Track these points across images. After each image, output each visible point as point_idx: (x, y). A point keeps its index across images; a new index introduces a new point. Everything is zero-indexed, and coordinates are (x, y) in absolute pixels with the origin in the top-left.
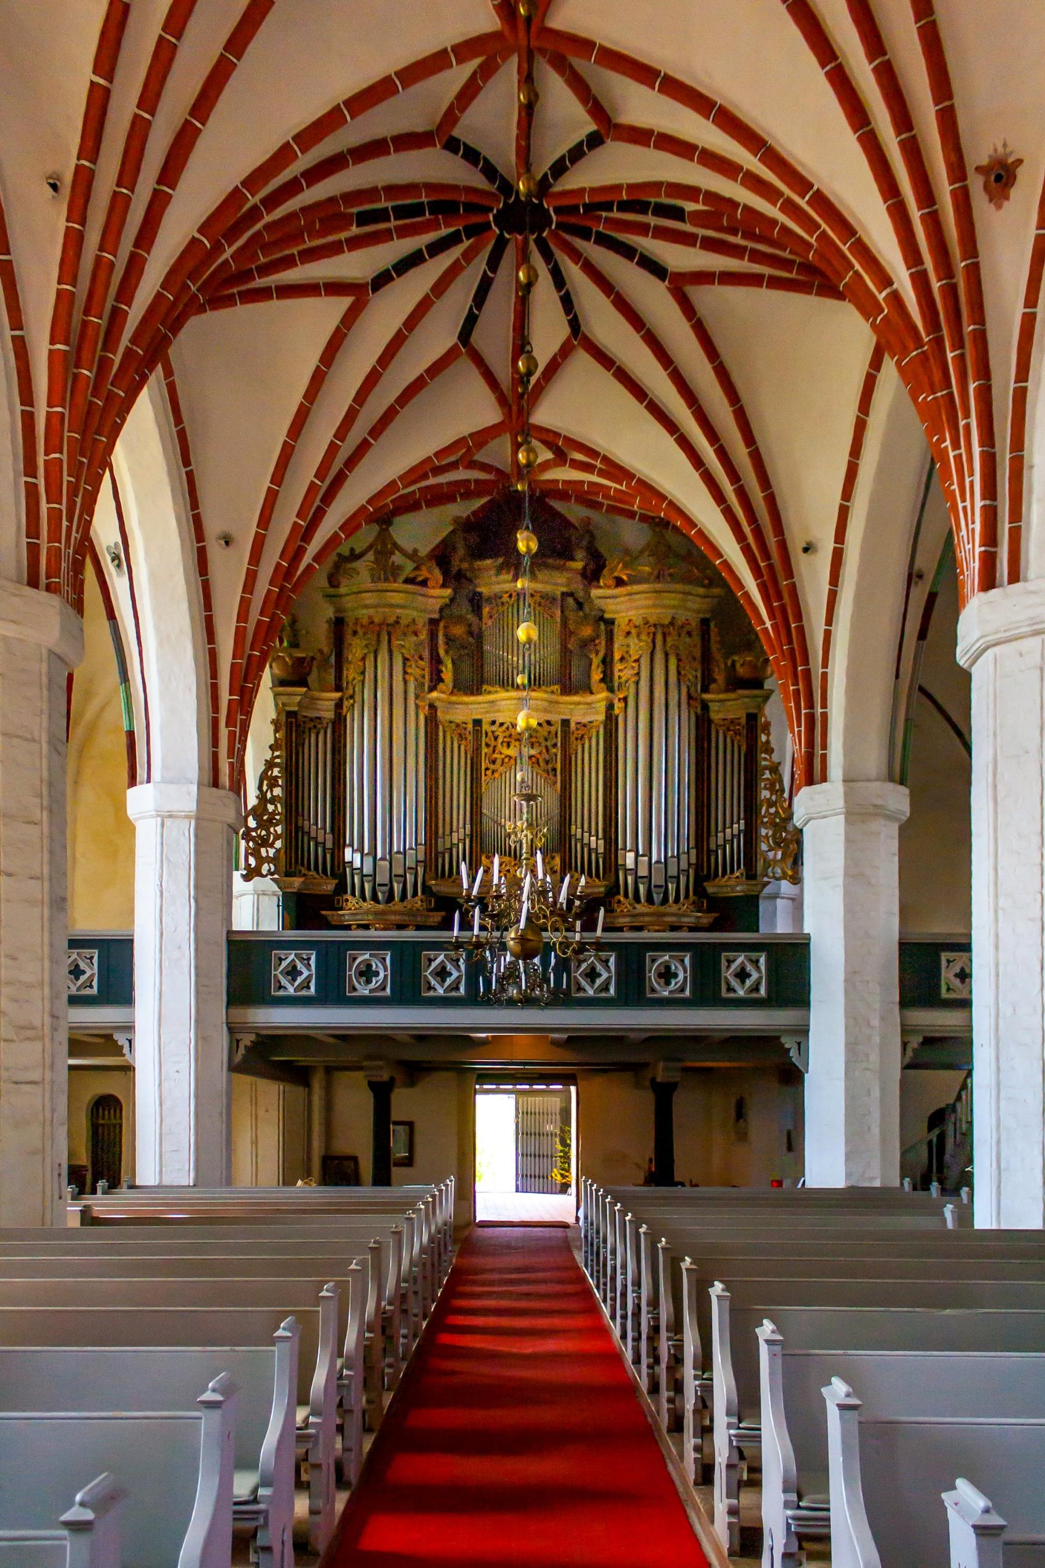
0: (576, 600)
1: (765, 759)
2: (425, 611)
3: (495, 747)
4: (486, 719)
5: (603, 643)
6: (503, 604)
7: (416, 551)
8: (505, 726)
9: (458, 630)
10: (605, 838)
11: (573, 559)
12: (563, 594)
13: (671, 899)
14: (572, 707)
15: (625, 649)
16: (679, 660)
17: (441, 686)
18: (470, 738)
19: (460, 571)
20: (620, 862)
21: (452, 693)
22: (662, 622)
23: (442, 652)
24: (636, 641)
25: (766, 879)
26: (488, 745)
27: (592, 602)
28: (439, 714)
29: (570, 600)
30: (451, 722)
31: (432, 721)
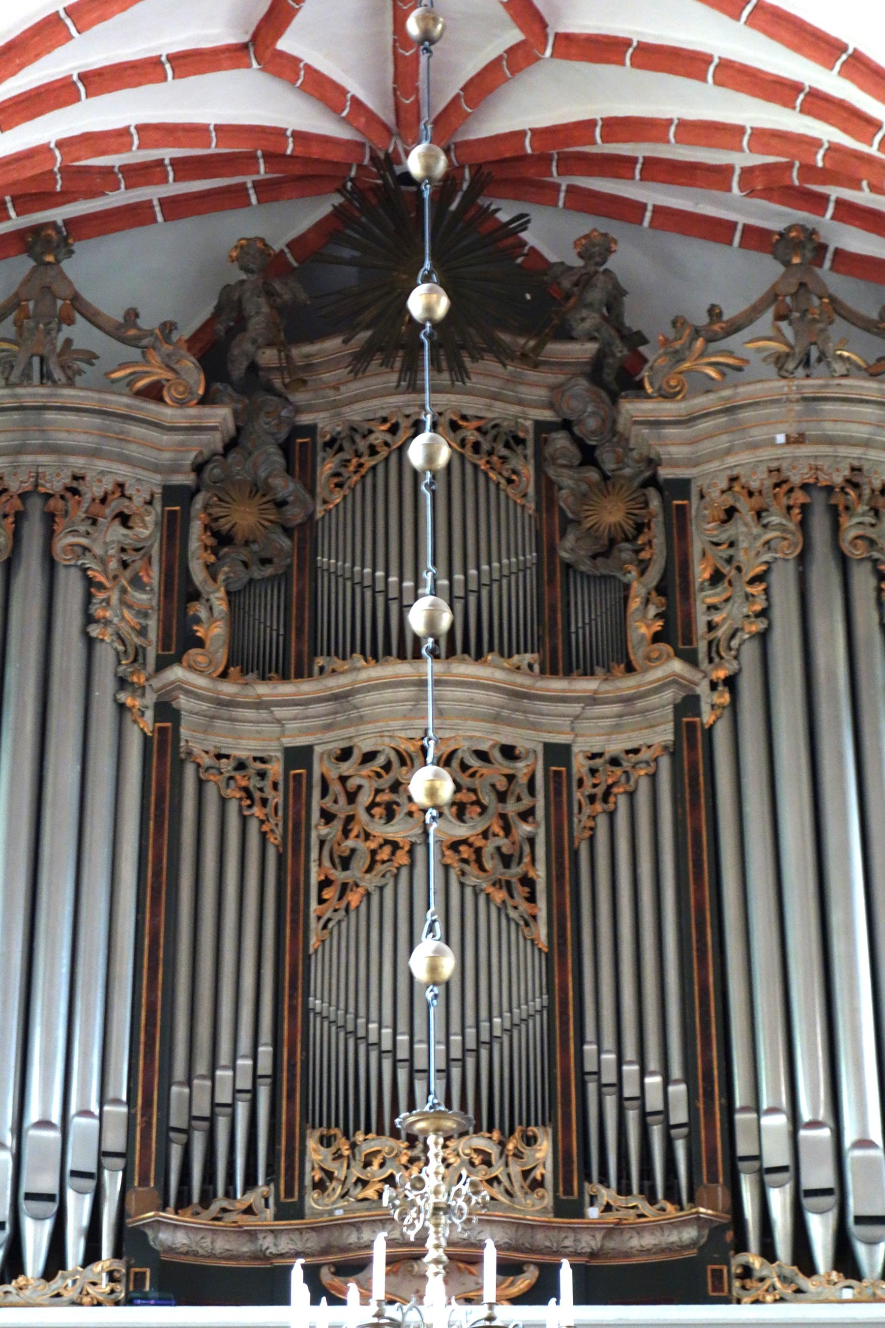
0: (579, 442)
2: (156, 468)
3: (350, 819)
4: (325, 744)
5: (659, 541)
6: (373, 451)
7: (132, 315)
8: (381, 760)
9: (244, 517)
10: (689, 1078)
11: (565, 334)
12: (541, 427)
14: (576, 708)
15: (724, 551)
17: (194, 654)
18: (276, 798)
19: (253, 368)
20: (743, 1148)
21: (224, 675)
23: (198, 574)
24: (756, 530)
26: (328, 817)
28: (184, 732)
29: (560, 441)
30: (219, 756)
31: (164, 752)
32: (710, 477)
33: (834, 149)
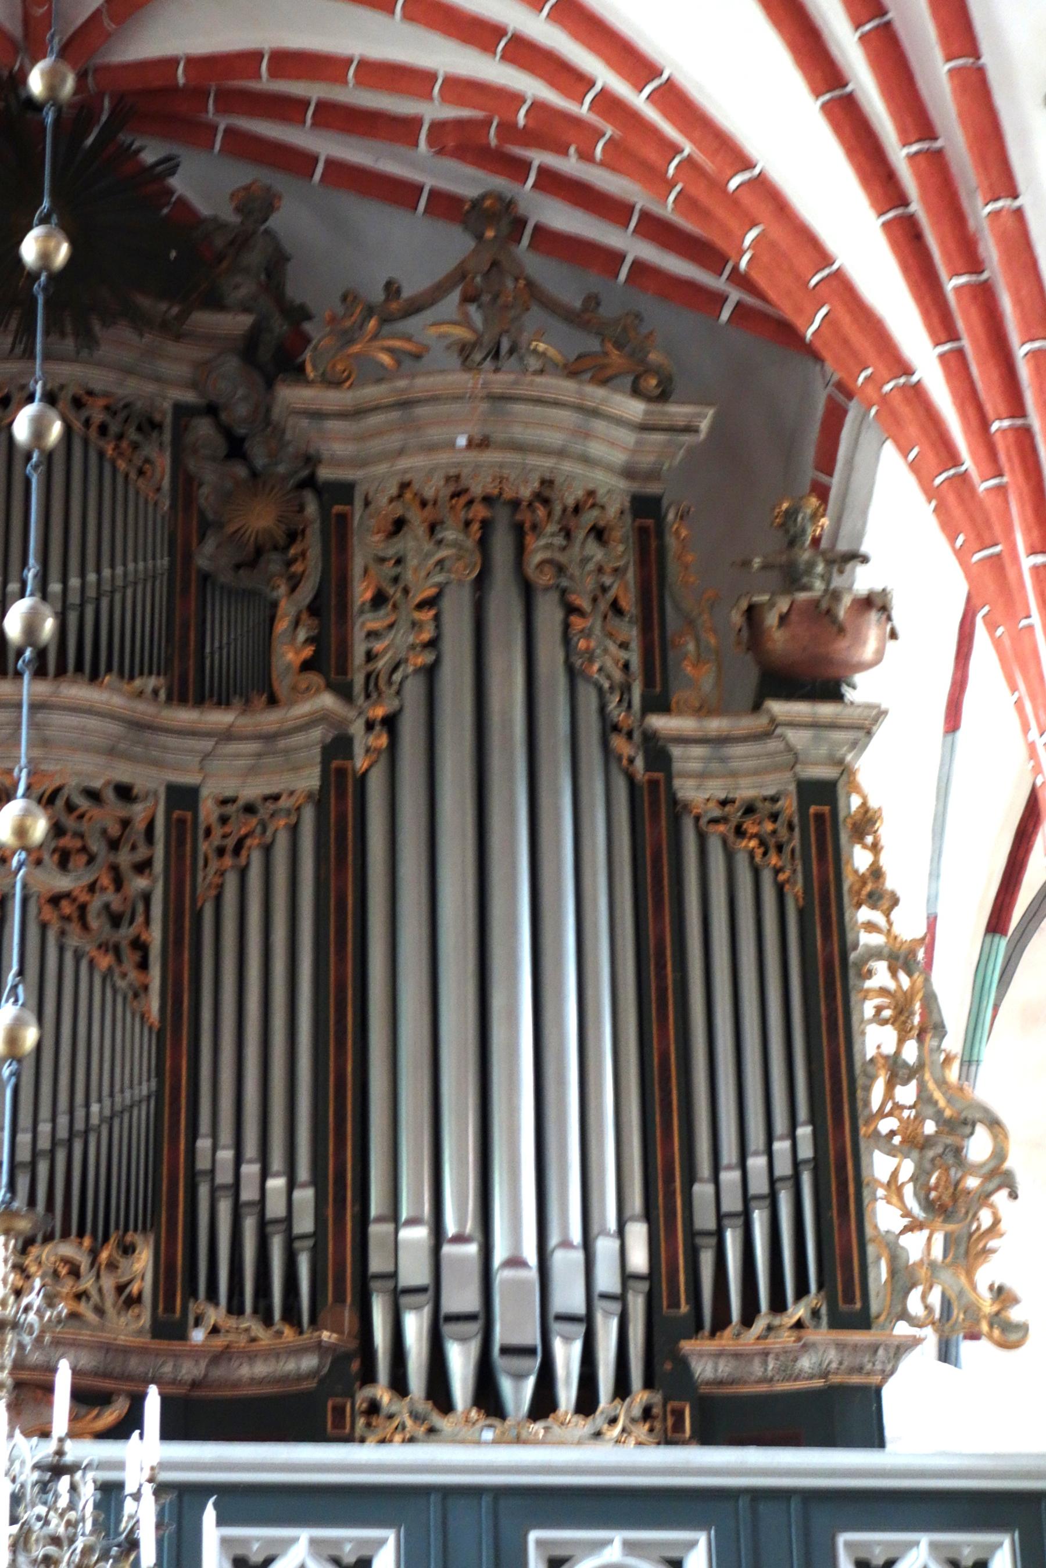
1: (871, 927)
5: (314, 553)
10: (317, 1180)
11: (215, 302)
12: (182, 411)
13: (567, 1394)
14: (208, 744)
15: (389, 569)
16: (571, 610)
20: (377, 1264)
22: (509, 494)
24: (427, 546)
25: (902, 1329)
27: (279, 431)
29: (203, 428)
32: (379, 480)
33: (538, 107)
